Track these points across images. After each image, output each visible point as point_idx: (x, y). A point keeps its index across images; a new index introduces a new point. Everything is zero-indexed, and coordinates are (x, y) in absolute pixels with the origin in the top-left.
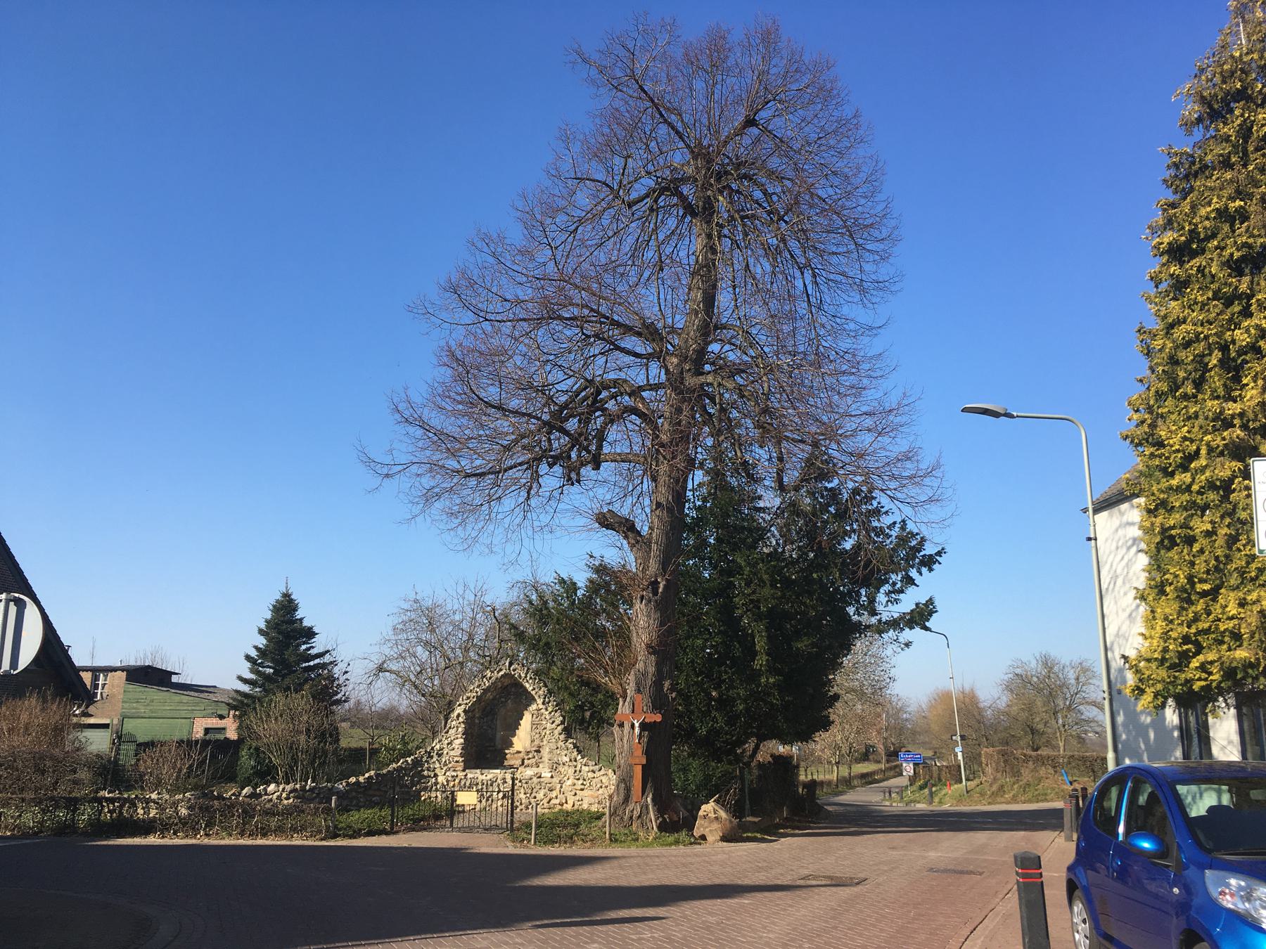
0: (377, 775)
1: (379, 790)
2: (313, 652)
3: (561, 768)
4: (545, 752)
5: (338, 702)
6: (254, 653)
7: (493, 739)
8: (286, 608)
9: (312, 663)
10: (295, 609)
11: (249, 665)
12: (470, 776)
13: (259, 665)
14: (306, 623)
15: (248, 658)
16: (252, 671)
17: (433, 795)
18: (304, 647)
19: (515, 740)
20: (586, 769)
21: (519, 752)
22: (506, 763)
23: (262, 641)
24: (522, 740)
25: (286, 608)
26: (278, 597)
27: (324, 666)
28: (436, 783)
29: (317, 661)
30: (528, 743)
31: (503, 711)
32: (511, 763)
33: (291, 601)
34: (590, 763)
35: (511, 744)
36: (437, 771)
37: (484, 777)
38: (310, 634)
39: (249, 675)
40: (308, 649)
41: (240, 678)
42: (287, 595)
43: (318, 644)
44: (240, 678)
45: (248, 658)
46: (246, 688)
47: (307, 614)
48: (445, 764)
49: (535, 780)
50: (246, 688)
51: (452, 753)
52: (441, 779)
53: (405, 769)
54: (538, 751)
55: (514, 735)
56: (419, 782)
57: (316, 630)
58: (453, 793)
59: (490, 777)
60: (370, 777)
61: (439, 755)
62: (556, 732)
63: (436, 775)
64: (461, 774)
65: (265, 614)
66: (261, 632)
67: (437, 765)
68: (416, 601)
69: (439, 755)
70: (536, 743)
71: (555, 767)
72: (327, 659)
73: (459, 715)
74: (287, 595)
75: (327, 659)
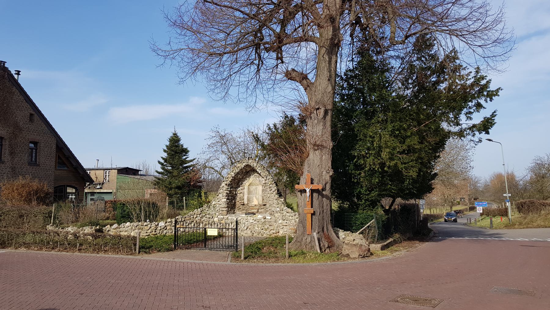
6: (162, 161)
8: (175, 140)
10: (179, 140)
11: (160, 166)
12: (229, 218)
14: (185, 147)
15: (159, 162)
16: (163, 169)
18: (184, 157)
23: (165, 155)
25: (175, 140)
26: (171, 135)
33: (177, 137)
38: (186, 151)
39: (160, 170)
42: (175, 134)
45: (159, 162)
47: (185, 143)
57: (189, 149)
58: (205, 229)
66: (165, 151)
74: (175, 134)
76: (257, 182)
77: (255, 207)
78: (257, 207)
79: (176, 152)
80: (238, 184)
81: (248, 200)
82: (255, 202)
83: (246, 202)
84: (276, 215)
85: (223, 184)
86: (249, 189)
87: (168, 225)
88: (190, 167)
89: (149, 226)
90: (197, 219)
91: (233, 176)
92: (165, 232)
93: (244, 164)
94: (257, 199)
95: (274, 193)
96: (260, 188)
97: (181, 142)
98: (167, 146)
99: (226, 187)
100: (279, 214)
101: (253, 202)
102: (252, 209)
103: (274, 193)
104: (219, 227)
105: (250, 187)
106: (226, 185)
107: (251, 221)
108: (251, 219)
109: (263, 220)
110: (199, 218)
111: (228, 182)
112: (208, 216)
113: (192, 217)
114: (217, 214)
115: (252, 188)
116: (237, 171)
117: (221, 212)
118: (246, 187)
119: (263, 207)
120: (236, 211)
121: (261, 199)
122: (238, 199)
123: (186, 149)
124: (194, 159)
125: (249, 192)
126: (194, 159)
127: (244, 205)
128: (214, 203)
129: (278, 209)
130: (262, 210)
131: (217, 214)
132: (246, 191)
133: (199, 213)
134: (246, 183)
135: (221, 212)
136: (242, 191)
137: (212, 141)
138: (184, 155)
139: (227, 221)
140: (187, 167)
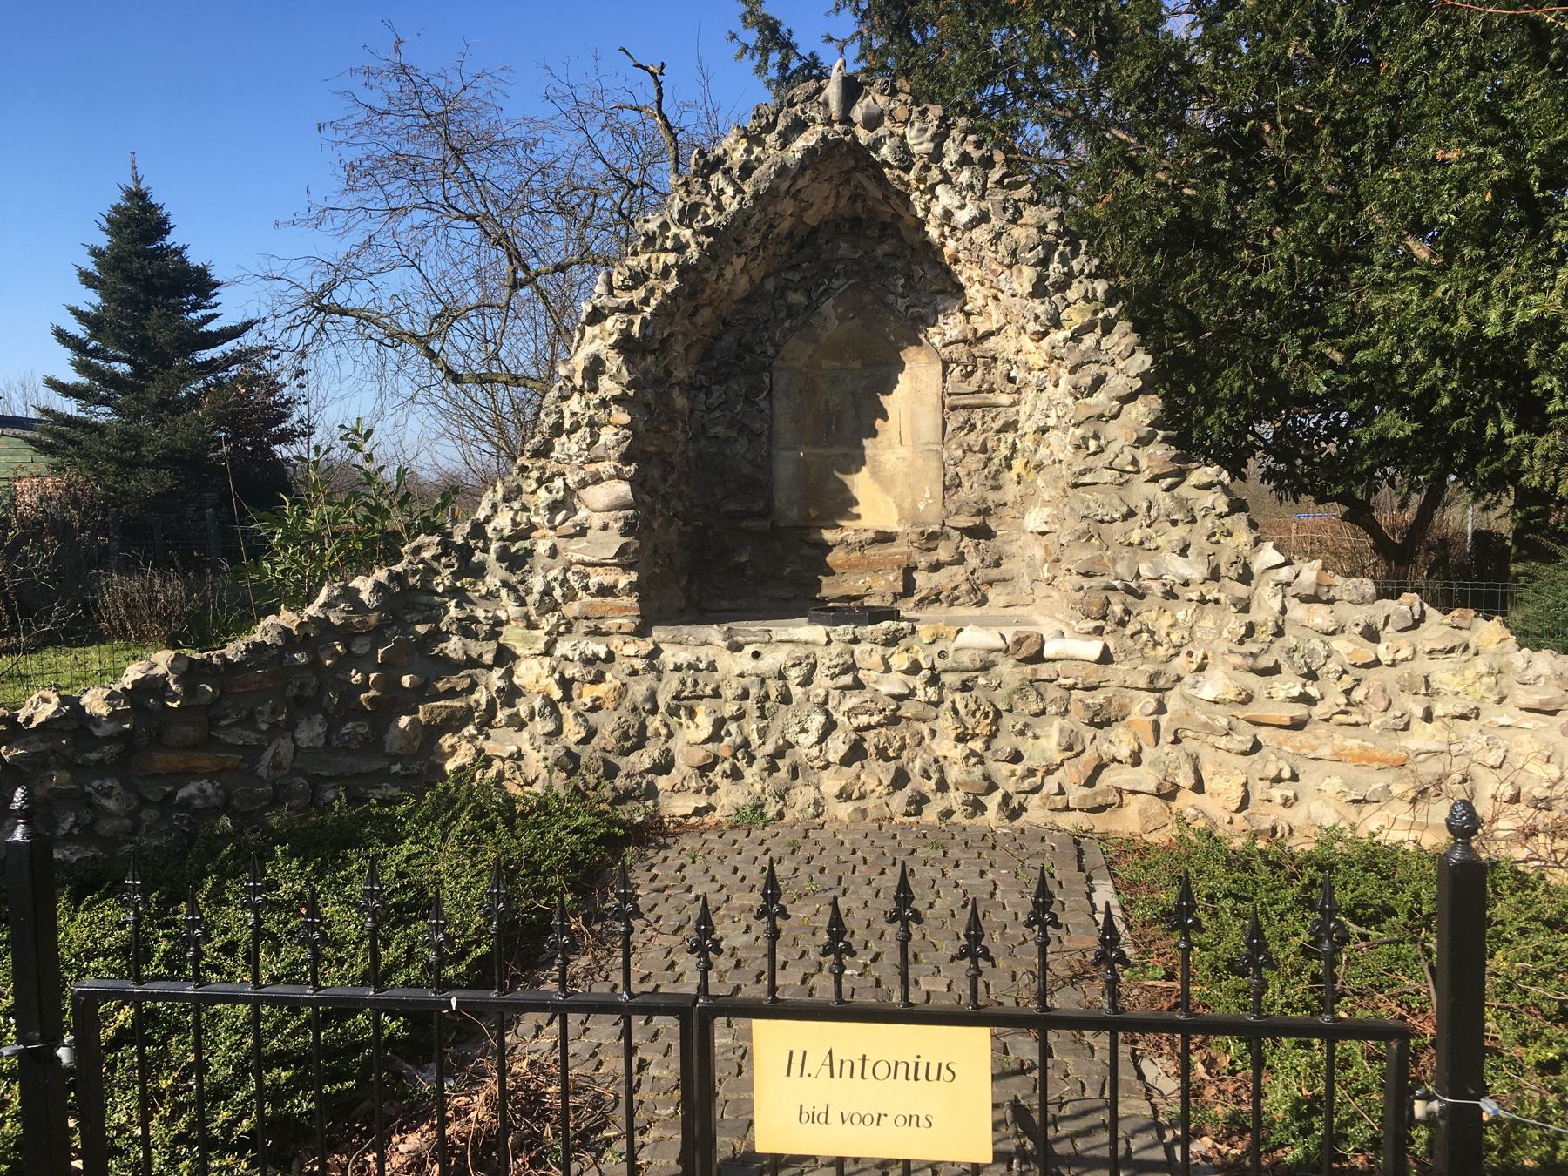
0: (190, 673)
1: (208, 743)
2: (213, 327)
3: (1150, 615)
4: (1033, 522)
5: (286, 437)
6: (78, 330)
7: (759, 485)
8: (139, 223)
10: (161, 227)
11: (67, 353)
12: (672, 655)
13: (94, 353)
14: (195, 258)
15: (62, 336)
16: (82, 368)
17: (501, 743)
19: (861, 484)
20: (1320, 616)
21: (885, 538)
22: (829, 589)
23: (90, 300)
24: (894, 481)
25: (139, 223)
26: (118, 198)
28: (511, 693)
29: (230, 346)
30: (928, 502)
31: (798, 353)
32: (853, 584)
33: (151, 208)
34: (1343, 586)
35: (844, 504)
36: (512, 636)
37: (744, 662)
38: (201, 284)
39: (71, 377)
41: (54, 384)
42: (138, 196)
44: (54, 384)
45: (62, 336)
46: (69, 407)
47: (195, 237)
48: (548, 603)
49: (1008, 672)
50: (69, 407)
51: (576, 550)
52: (531, 673)
53: (346, 633)
54: (981, 533)
55: (856, 461)
56: (424, 692)
57: (216, 274)
59: (774, 659)
60: (149, 687)
61: (516, 561)
62: (1119, 434)
63: (505, 657)
64: (631, 650)
65: (85, 234)
66: (87, 279)
67: (508, 608)
69: (516, 561)
70: (970, 492)
71: (1113, 606)
72: (250, 339)
73: (595, 367)
74: (138, 196)
75: (250, 339)
77: (874, 553)
88: (229, 361)
98: (95, 252)
104: (1007, 983)
107: (893, 684)
124: (249, 325)
126: (249, 325)
138: (196, 307)
140: (211, 366)
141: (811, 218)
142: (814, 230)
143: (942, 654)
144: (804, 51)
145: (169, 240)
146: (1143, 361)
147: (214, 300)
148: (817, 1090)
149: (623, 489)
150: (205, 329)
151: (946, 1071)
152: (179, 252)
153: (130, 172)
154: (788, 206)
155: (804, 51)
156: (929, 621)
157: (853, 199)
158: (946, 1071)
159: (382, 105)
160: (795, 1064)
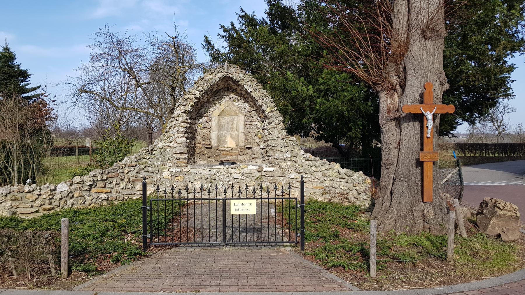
2: (28, 87)
5: (51, 119)
9: (29, 94)
10: (13, 58)
14: (22, 68)
18: (23, 83)
27: (37, 96)
29: (33, 93)
33: (11, 53)
38: (25, 75)
40: (26, 85)
42: (6, 49)
43: (32, 82)
57: (29, 72)
58: (224, 200)
68: (109, 35)
72: (39, 91)
74: (6, 49)
75: (39, 91)
76: (235, 109)
77: (231, 152)
78: (236, 152)
79: (10, 76)
80: (198, 113)
81: (219, 140)
82: (230, 143)
83: (214, 143)
84: (283, 165)
85: (178, 111)
86: (219, 120)
87: (76, 189)
88: (33, 97)
89: (37, 192)
90: (130, 174)
91: (198, 96)
92: (70, 202)
93: (220, 75)
94: (236, 139)
95: (279, 127)
96: (242, 119)
97: (17, 62)
99: (185, 116)
100: (289, 163)
101: (226, 143)
102: (226, 155)
103: (279, 127)
105: (221, 118)
106: (185, 112)
107: (236, 176)
108: (234, 173)
109: (257, 174)
110: (134, 173)
111: (188, 108)
112: (150, 169)
113: (121, 171)
114: (169, 164)
115: (225, 119)
116: (206, 87)
117: (175, 161)
118: (214, 118)
119: (246, 151)
120: (197, 158)
121: (242, 138)
122: (199, 138)
123: (25, 71)
124: (39, 87)
125: (220, 127)
126: (39, 87)
127: (211, 148)
128: (160, 145)
129: (288, 155)
130: (245, 157)
131: (169, 164)
132: (214, 124)
133: (135, 164)
134: (215, 111)
135: (175, 161)
136: (206, 125)
137: (98, 50)
138: (23, 81)
139: (187, 177)
140: (28, 98)
141: (220, 88)
142: (220, 90)
143: (245, 171)
144: (216, 48)
145: (15, 62)
146: (281, 118)
147: (28, 79)
148: (238, 207)
149: (185, 139)
150: (27, 87)
151: (251, 204)
152: (19, 65)
153: (5, 42)
154: (216, 87)
155: (216, 48)
156: (242, 165)
157: (228, 84)
158: (251, 204)
159: (102, 41)
160: (235, 204)
